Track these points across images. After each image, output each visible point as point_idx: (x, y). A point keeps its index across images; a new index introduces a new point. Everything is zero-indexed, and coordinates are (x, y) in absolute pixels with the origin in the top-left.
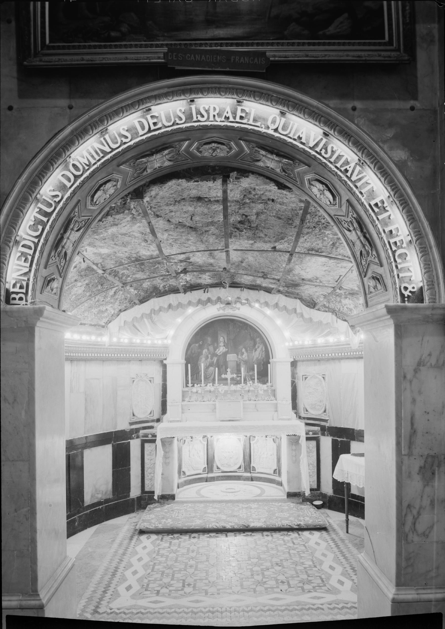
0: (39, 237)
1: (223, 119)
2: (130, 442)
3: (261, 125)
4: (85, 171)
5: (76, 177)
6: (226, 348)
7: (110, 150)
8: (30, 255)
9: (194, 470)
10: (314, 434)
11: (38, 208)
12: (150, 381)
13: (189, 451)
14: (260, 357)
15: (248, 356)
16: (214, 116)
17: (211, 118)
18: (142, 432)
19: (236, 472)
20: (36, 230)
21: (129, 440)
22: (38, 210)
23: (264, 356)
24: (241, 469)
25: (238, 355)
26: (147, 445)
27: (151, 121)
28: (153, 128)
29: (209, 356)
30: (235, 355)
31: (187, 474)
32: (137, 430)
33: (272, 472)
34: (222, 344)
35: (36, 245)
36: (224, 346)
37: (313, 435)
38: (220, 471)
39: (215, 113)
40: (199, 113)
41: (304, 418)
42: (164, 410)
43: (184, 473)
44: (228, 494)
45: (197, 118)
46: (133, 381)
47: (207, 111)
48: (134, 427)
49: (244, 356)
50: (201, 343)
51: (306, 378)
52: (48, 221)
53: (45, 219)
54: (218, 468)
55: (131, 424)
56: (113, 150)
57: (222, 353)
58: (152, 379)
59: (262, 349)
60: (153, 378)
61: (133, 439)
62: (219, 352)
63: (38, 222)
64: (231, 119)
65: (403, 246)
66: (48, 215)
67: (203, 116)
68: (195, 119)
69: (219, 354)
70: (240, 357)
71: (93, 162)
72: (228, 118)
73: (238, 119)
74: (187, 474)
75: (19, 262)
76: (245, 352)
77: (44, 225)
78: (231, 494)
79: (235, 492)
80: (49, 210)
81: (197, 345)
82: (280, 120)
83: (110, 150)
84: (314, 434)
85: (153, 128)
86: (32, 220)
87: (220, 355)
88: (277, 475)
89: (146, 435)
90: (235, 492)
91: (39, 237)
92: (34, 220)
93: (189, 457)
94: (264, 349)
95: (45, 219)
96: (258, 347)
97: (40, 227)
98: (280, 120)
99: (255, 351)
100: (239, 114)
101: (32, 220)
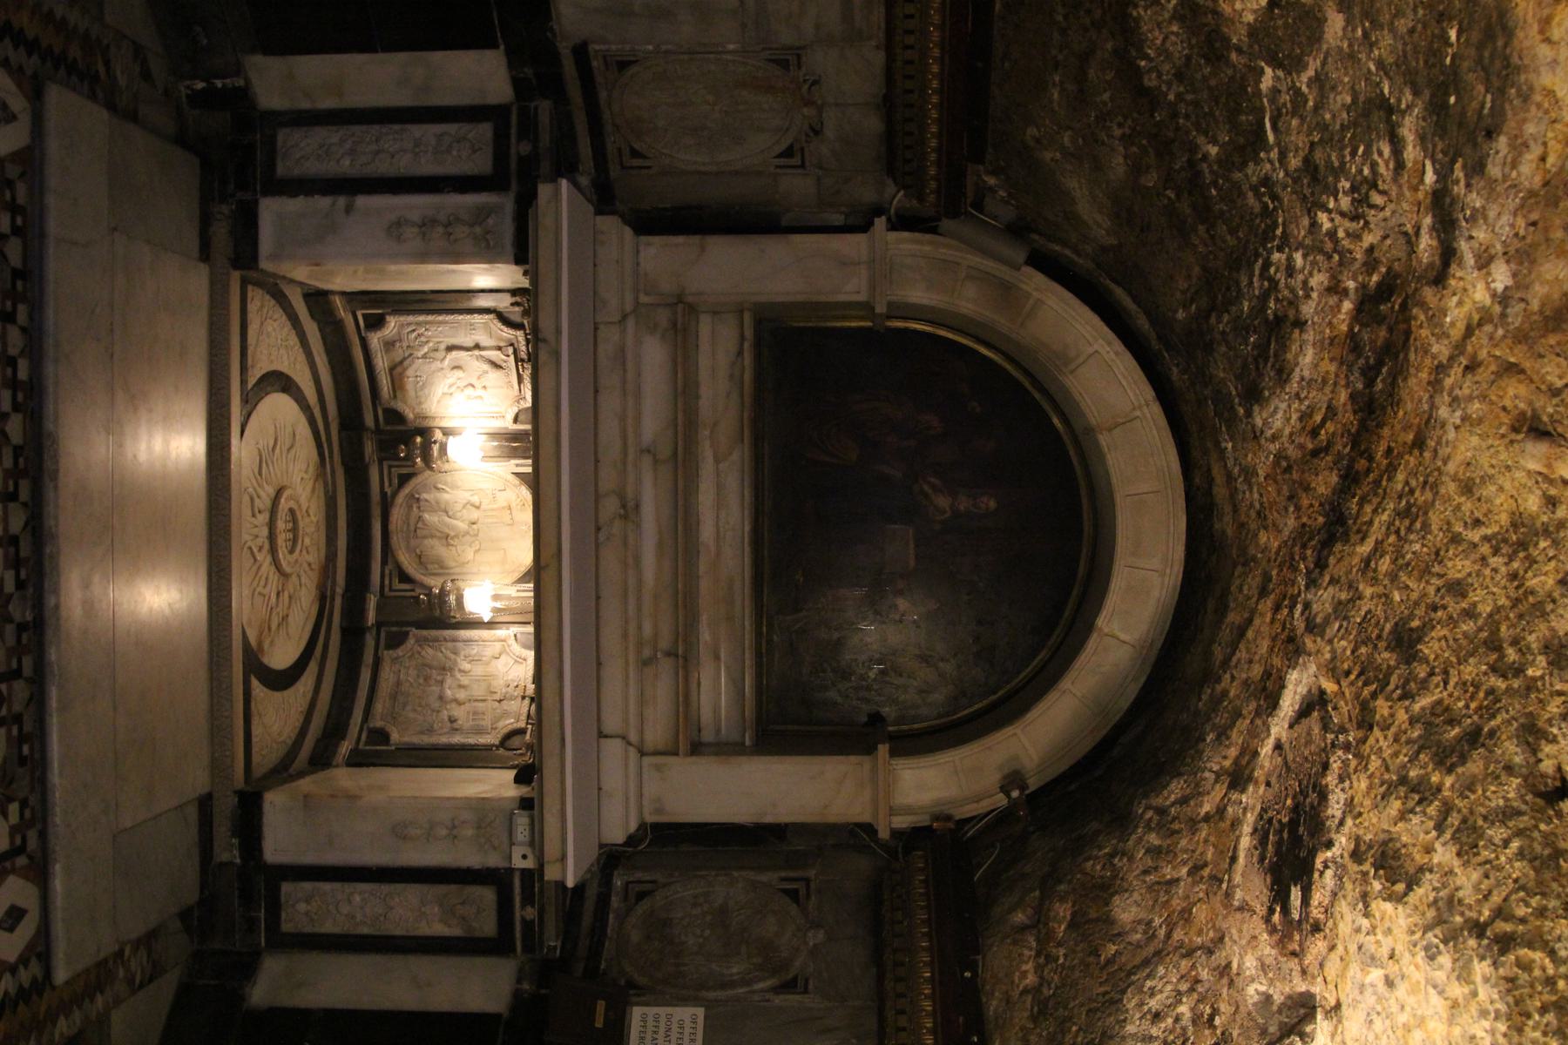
2: (495, 46)
9: (392, 369)
10: (527, 925)
12: (788, 153)
13: (477, 347)
18: (544, 109)
19: (384, 562)
21: (502, 47)
24: (397, 585)
26: (485, 130)
30: (912, 563)
31: (375, 339)
32: (551, 85)
33: (377, 723)
34: (964, 504)
37: (523, 920)
38: (388, 490)
41: (606, 881)
42: (648, 223)
43: (376, 323)
44: (263, 518)
46: (783, 64)
48: (569, 67)
51: (793, 895)
54: (404, 479)
55: (581, 51)
60: (803, 166)
61: (511, 65)
62: (926, 488)
74: (375, 339)
78: (265, 532)
79: (273, 550)
84: (527, 925)
88: (361, 746)
89: (528, 127)
90: (273, 550)
93: (450, 348)
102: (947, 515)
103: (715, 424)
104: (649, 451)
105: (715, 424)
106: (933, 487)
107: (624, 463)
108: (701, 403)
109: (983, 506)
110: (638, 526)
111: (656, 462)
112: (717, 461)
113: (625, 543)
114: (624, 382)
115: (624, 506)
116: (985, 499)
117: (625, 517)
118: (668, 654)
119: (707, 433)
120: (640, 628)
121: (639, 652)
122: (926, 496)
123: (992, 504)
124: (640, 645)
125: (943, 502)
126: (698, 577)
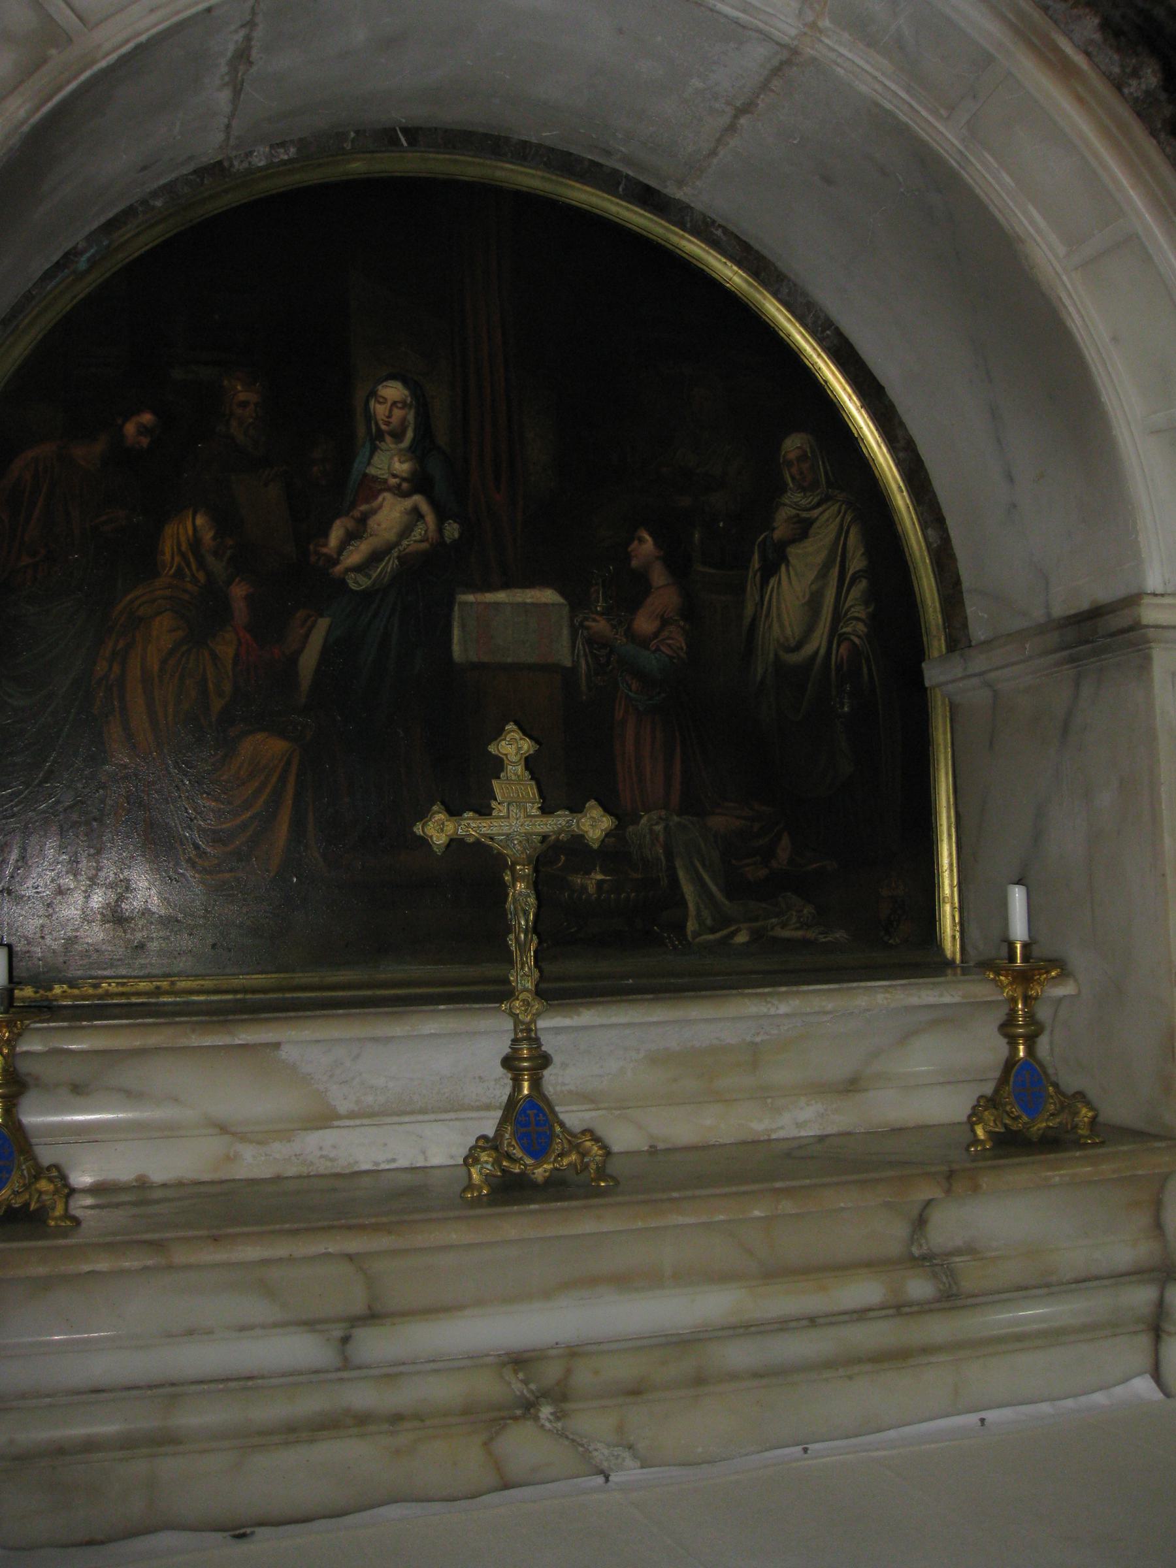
6: (442, 516)
14: (818, 641)
15: (690, 612)
23: (856, 629)
25: (577, 602)
29: (239, 591)
30: (548, 596)
36: (420, 483)
49: (644, 624)
57: (390, 565)
59: (837, 555)
62: (355, 555)
69: (359, 583)
70: (600, 625)
76: (659, 576)
87: (367, 595)
94: (857, 563)
96: (803, 529)
99: (770, 570)
102: (425, 507)
103: (223, 1129)
104: (345, 1340)
105: (223, 1129)
106: (352, 537)
107: (396, 1418)
108: (157, 1176)
109: (398, 413)
110: (574, 1352)
111: (373, 1316)
112: (325, 1119)
113: (635, 1391)
114: (128, 1444)
115: (528, 1407)
116: (380, 410)
117: (560, 1395)
118: (920, 1223)
119: (248, 1153)
120: (861, 1314)
121: (923, 1309)
122: (375, 557)
123: (393, 391)
124: (899, 1308)
126: (653, 1151)
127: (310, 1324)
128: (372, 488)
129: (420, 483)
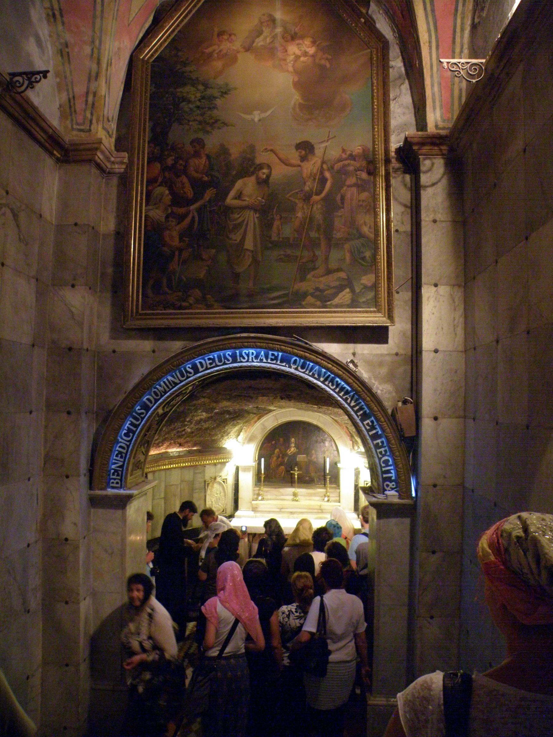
0: (130, 441)
1: (258, 361)
3: (286, 365)
4: (162, 396)
5: (156, 401)
6: (297, 449)
7: (179, 382)
8: (124, 453)
11: (130, 421)
16: (252, 358)
17: (250, 360)
20: (129, 436)
22: (130, 422)
27: (208, 362)
28: (209, 366)
35: (128, 446)
36: (295, 447)
39: (253, 356)
40: (241, 356)
45: (240, 359)
47: (248, 355)
50: (273, 442)
52: (137, 430)
53: (134, 429)
56: (181, 381)
58: (225, 480)
60: (226, 479)
63: (129, 430)
64: (265, 360)
65: (387, 454)
66: (137, 426)
67: (244, 358)
68: (239, 360)
69: (290, 455)
71: (167, 390)
72: (262, 360)
73: (269, 361)
75: (116, 458)
77: (134, 433)
80: (138, 423)
81: (270, 444)
82: (300, 361)
83: (179, 382)
85: (209, 366)
86: (125, 429)
87: (290, 456)
91: (130, 441)
92: (127, 429)
95: (134, 429)
97: (131, 435)
98: (300, 361)
100: (270, 356)
101: (125, 429)
112: (283, 495)
123: (293, 439)
125: (292, 449)
127: (278, 508)
128: (291, 447)
129: (295, 447)
